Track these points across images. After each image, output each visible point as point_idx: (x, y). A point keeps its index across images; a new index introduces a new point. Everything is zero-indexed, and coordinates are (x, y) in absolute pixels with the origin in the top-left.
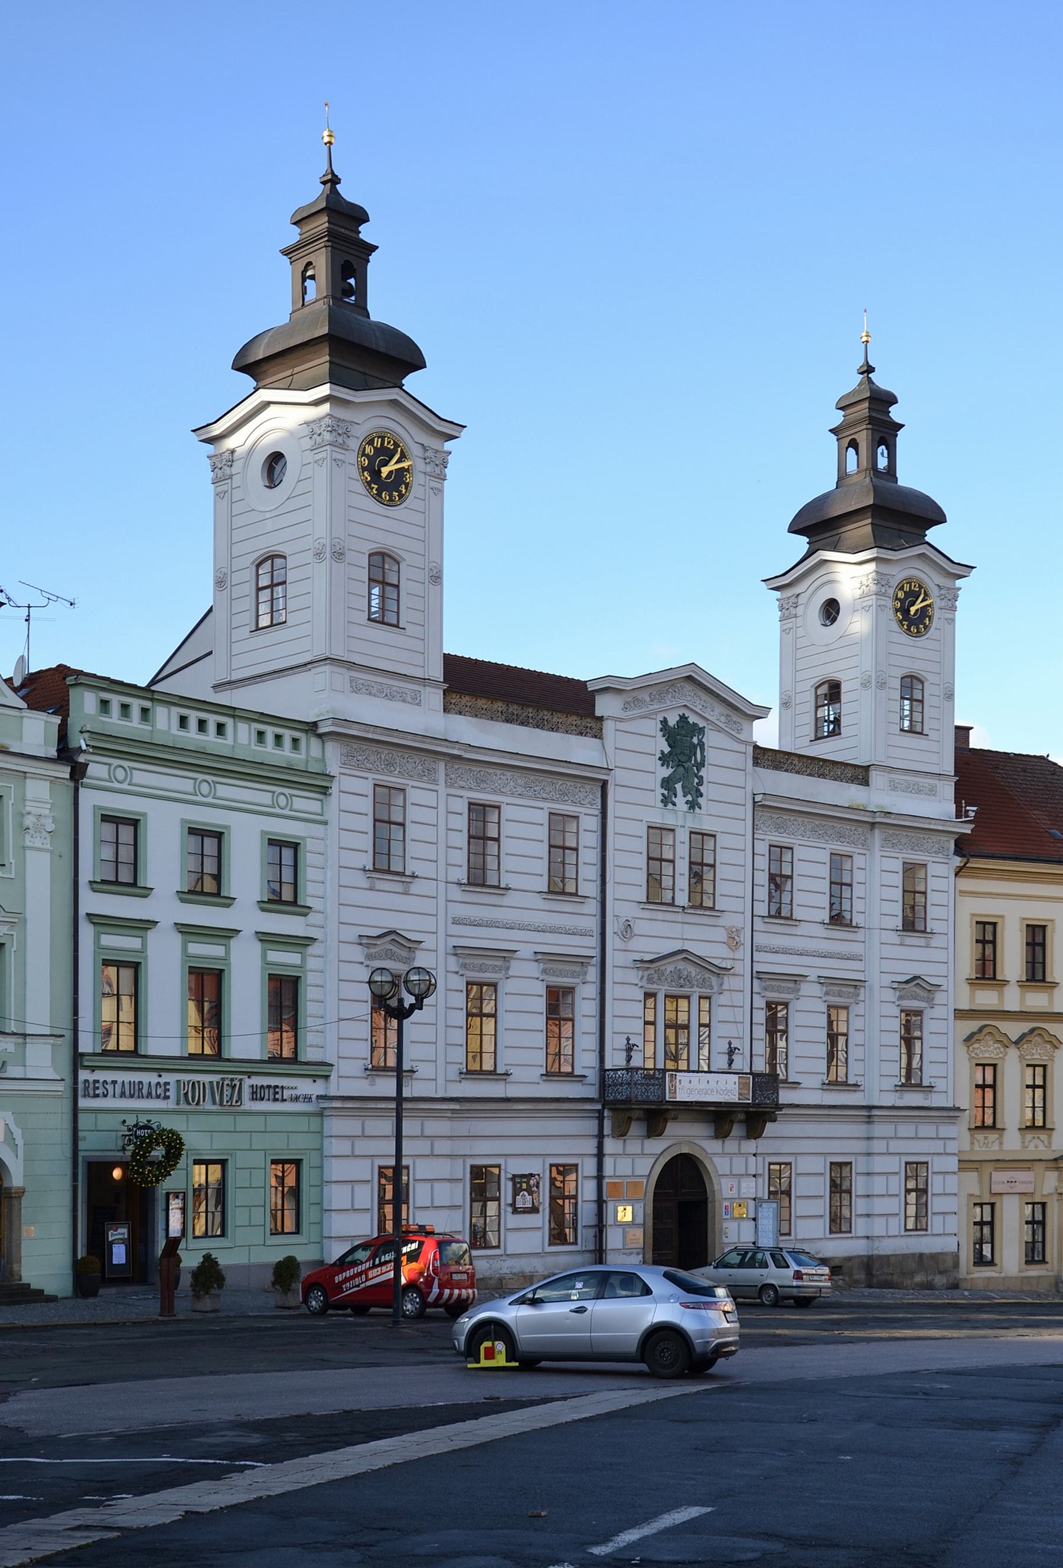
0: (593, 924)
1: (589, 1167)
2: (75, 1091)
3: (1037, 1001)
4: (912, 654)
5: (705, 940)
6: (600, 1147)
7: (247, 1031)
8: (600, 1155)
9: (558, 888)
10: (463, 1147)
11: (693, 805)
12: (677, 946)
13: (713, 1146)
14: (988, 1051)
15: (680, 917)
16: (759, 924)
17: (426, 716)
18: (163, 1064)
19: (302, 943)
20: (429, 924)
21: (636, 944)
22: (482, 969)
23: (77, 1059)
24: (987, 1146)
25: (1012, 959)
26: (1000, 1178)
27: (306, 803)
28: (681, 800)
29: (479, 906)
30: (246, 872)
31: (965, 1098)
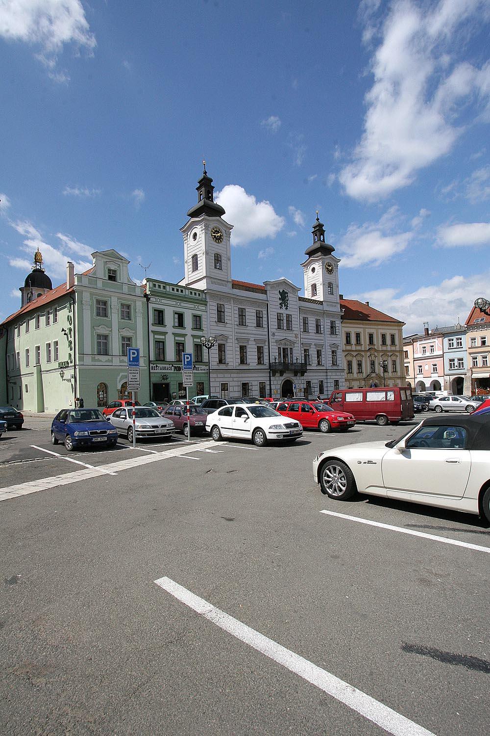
0: (267, 333)
1: (268, 383)
2: (150, 369)
3: (358, 348)
4: (331, 278)
5: (290, 336)
6: (270, 378)
8: (270, 380)
9: (259, 325)
10: (240, 379)
11: (286, 309)
12: (285, 338)
13: (294, 378)
14: (349, 358)
15: (285, 332)
17: (228, 289)
20: (231, 333)
21: (275, 337)
22: (243, 343)
23: (150, 362)
24: (350, 376)
25: (353, 340)
28: (284, 307)
29: (242, 329)
30: (188, 321)
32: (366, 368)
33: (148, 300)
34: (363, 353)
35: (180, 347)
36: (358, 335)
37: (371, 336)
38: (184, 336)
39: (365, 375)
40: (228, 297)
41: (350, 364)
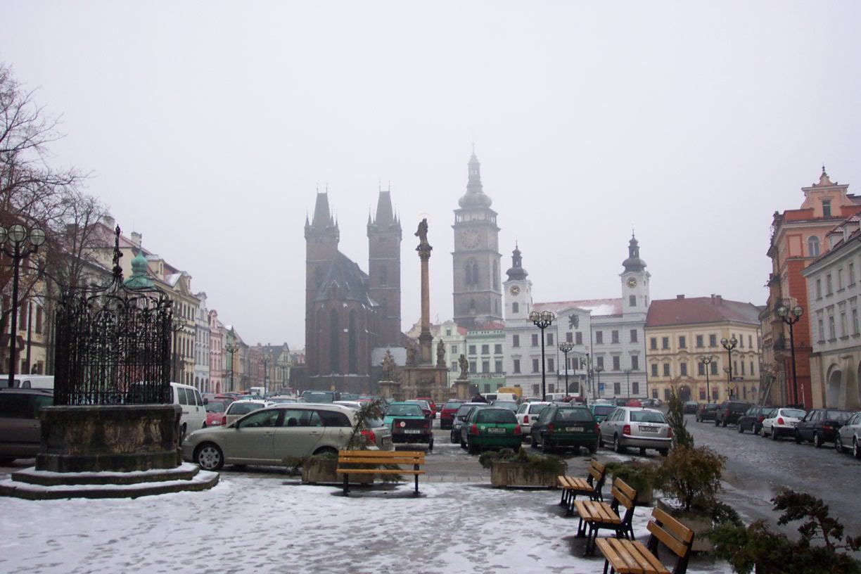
3: (666, 352)
7: (492, 368)
14: (655, 362)
16: (593, 345)
18: (480, 373)
19: (502, 357)
26: (658, 386)
27: (503, 339)
30: (492, 349)
31: (650, 371)
32: (675, 371)
33: (465, 341)
34: (672, 357)
35: (486, 364)
36: (665, 340)
37: (682, 340)
38: (489, 358)
39: (673, 378)
40: (522, 329)
41: (655, 367)
